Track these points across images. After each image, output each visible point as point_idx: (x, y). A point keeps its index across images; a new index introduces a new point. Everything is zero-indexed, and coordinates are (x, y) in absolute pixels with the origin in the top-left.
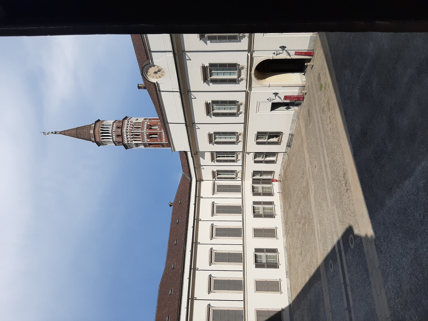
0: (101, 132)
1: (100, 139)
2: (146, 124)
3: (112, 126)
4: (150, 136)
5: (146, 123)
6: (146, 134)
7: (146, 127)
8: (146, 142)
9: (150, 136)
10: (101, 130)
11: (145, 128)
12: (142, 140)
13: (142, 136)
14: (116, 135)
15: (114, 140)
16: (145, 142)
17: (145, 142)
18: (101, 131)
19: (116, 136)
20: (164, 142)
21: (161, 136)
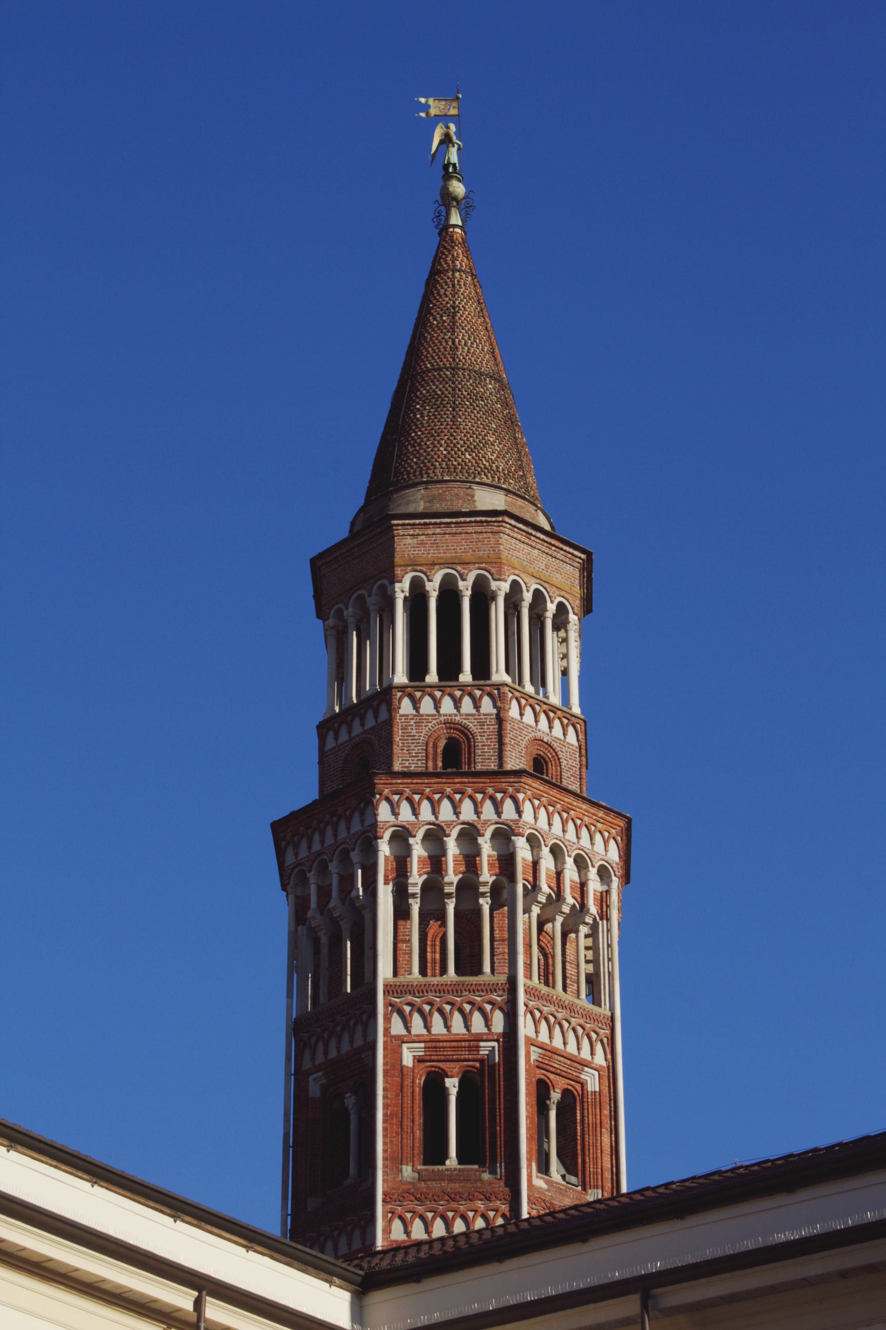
0: (494, 585)
1: (413, 564)
2: (585, 1054)
3: (555, 699)
4: (452, 1084)
5: (600, 1059)
6: (479, 1038)
7: (558, 1043)
8: (387, 1031)
9: (452, 1084)
10: (515, 586)
11: (544, 1037)
12: (409, 989)
13: (456, 989)
14: (464, 731)
15: (406, 707)
16: (387, 1019)
17: (387, 1019)
18: (505, 587)
19: (450, 724)
20: (387, 1231)
21: (453, 1197)
